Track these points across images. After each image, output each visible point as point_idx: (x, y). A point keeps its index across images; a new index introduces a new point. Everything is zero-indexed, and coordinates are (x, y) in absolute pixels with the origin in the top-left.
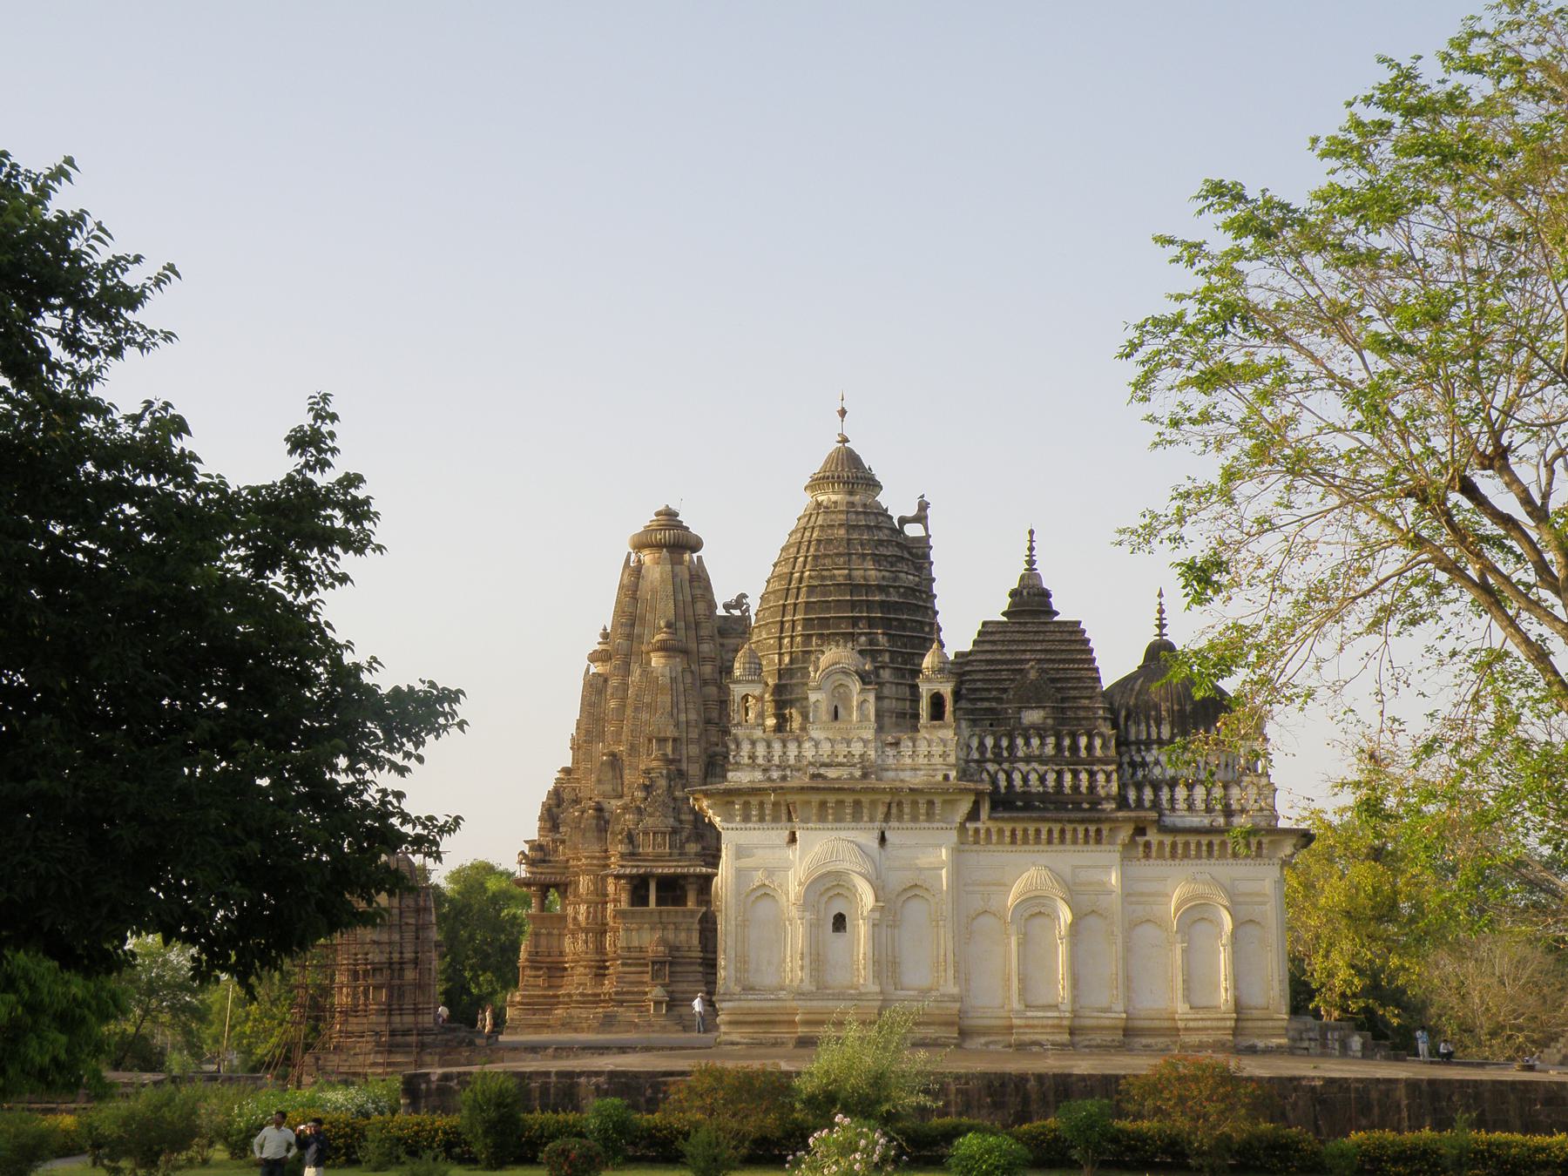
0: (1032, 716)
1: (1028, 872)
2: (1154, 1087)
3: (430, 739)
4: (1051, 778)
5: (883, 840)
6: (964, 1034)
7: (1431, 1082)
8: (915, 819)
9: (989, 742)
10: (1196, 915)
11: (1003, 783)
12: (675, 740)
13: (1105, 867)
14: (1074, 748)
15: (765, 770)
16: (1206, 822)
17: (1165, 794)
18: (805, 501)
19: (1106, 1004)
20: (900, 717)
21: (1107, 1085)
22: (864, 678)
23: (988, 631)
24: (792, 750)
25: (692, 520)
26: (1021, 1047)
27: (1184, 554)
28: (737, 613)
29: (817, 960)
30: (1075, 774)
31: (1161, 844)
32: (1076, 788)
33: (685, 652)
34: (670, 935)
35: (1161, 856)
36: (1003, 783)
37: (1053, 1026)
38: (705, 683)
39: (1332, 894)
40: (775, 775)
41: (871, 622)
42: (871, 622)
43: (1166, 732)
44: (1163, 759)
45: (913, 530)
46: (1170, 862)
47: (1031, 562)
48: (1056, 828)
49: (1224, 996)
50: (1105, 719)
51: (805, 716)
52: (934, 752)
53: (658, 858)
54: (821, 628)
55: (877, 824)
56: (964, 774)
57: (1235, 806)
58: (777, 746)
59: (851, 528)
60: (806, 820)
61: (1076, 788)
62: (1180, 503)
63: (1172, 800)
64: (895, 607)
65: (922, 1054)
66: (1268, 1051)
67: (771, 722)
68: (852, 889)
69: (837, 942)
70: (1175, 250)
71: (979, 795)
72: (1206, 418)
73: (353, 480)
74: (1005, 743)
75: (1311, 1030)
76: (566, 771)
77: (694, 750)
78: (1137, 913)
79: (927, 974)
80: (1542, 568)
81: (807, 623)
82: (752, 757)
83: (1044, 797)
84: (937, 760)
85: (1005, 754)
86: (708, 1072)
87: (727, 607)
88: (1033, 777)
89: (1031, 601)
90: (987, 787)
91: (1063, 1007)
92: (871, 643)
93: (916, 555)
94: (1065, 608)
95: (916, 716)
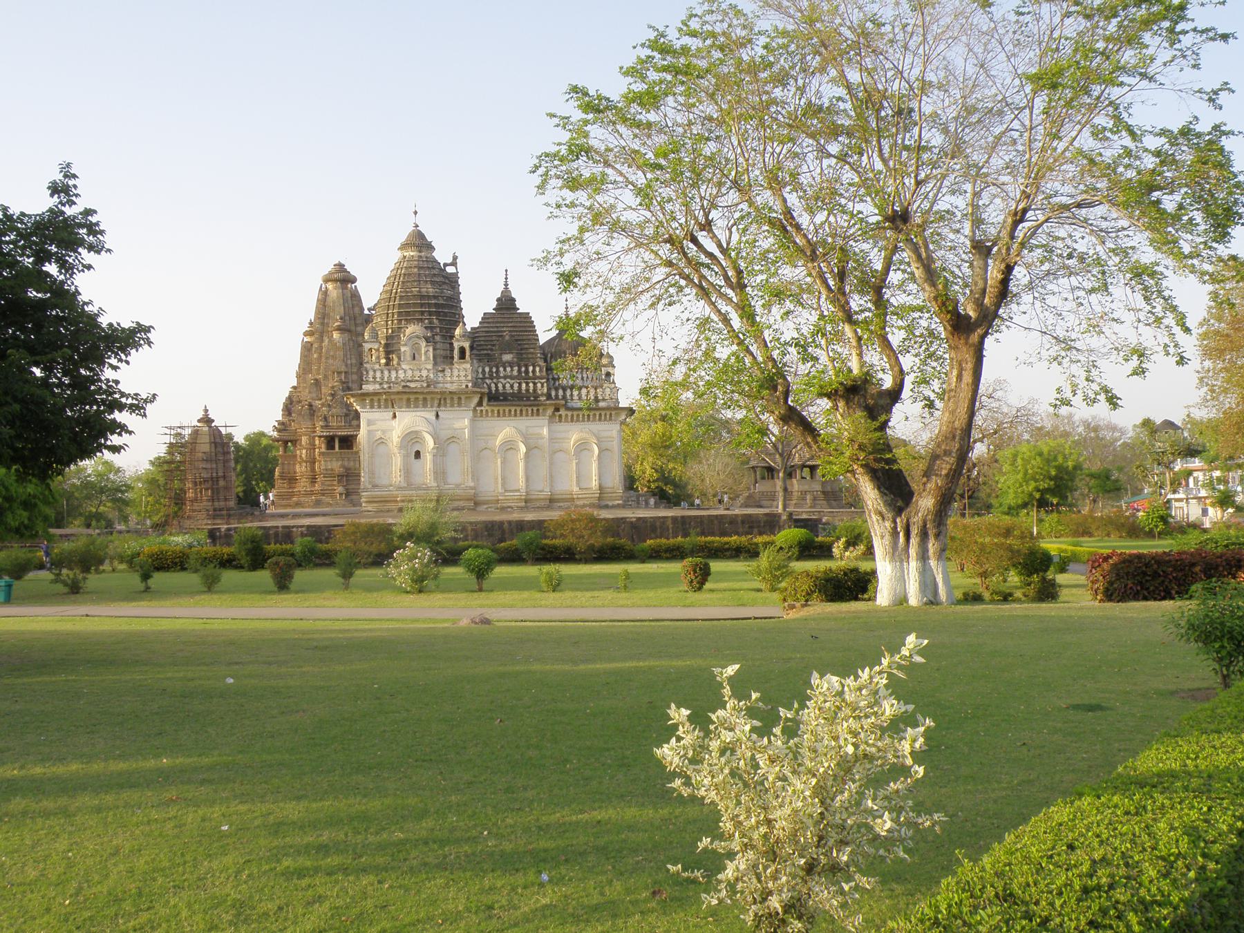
0: (507, 357)
1: (506, 429)
2: (560, 524)
3: (133, 351)
4: (516, 386)
5: (437, 416)
6: (477, 504)
7: (683, 517)
8: (452, 406)
9: (487, 369)
10: (582, 447)
13: (541, 427)
14: (527, 372)
18: (398, 255)
19: (542, 489)
20: (445, 358)
21: (539, 524)
22: (427, 340)
23: (486, 317)
24: (394, 374)
25: (352, 269)
26: (503, 509)
27: (561, 270)
29: (407, 472)
30: (527, 384)
32: (527, 390)
33: (349, 331)
34: (346, 463)
35: (566, 421)
39: (644, 436)
41: (430, 313)
42: (430, 313)
45: (450, 270)
47: (506, 285)
48: (518, 409)
49: (594, 484)
51: (399, 358)
52: (461, 374)
53: (339, 428)
54: (407, 316)
56: (475, 385)
58: (386, 373)
59: (420, 268)
61: (527, 390)
62: (559, 245)
63: (572, 395)
64: (442, 306)
65: (455, 513)
66: (613, 507)
67: (383, 361)
68: (423, 439)
69: (416, 464)
70: (556, 121)
71: (482, 394)
72: (573, 205)
73: (88, 212)
76: (294, 388)
78: (555, 448)
79: (459, 477)
80: (727, 278)
81: (400, 314)
83: (513, 395)
86: (353, 524)
87: (369, 309)
88: (508, 386)
89: (506, 303)
90: (486, 390)
93: (451, 282)
94: (522, 307)
95: (452, 358)
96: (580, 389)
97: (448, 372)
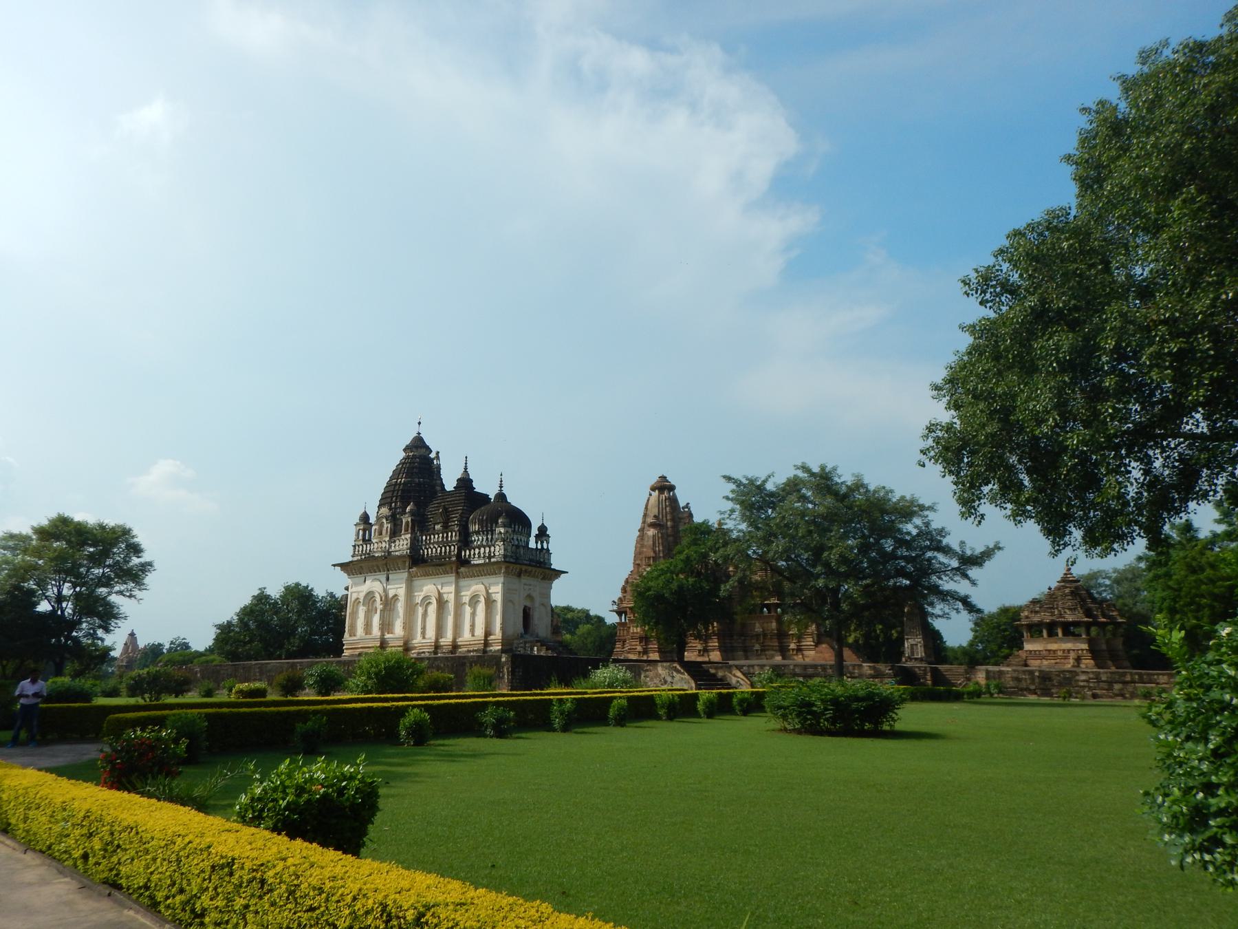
0: (438, 527)
1: (428, 588)
5: (388, 579)
25: (672, 480)
47: (466, 469)
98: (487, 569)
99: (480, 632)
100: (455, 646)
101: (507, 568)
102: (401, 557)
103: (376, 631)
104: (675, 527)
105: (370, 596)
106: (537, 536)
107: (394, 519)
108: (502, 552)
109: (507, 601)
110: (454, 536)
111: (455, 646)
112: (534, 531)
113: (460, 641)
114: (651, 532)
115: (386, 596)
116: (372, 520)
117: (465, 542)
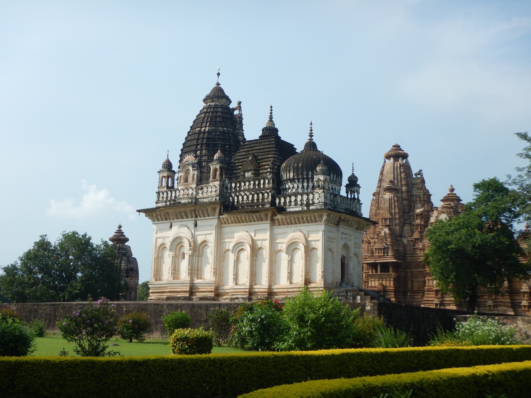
0: (248, 175)
1: (240, 234)
4: (251, 196)
5: (196, 225)
9: (233, 185)
11: (236, 200)
12: (390, 219)
14: (259, 184)
15: (166, 202)
16: (300, 209)
17: (288, 199)
25: (405, 149)
28: (419, 176)
31: (282, 220)
34: (384, 283)
36: (236, 200)
37: (243, 292)
38: (403, 200)
40: (168, 203)
43: (292, 174)
44: (291, 186)
46: (287, 226)
47: (271, 118)
50: (270, 172)
53: (380, 257)
55: (194, 219)
57: (311, 202)
58: (169, 193)
60: (173, 219)
61: (258, 199)
63: (290, 202)
74: (238, 185)
75: (343, 292)
77: (397, 221)
82: (163, 198)
84: (214, 193)
85: (238, 189)
87: (416, 175)
88: (245, 197)
91: (246, 285)
92: (201, 153)
96: (296, 195)
97: (205, 190)
98: (307, 216)
99: (299, 279)
100: (271, 293)
101: (329, 215)
102: (210, 203)
103: (184, 276)
104: (409, 191)
105: (177, 242)
106: (347, 186)
107: (199, 166)
108: (322, 199)
109: (328, 250)
110: (267, 183)
111: (271, 293)
112: (345, 181)
113: (276, 288)
114: (388, 196)
115: (195, 242)
116: (175, 168)
117: (279, 188)
